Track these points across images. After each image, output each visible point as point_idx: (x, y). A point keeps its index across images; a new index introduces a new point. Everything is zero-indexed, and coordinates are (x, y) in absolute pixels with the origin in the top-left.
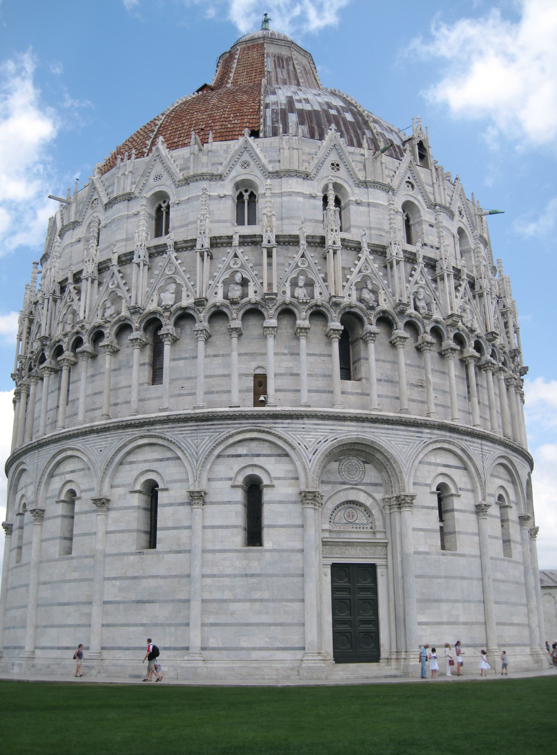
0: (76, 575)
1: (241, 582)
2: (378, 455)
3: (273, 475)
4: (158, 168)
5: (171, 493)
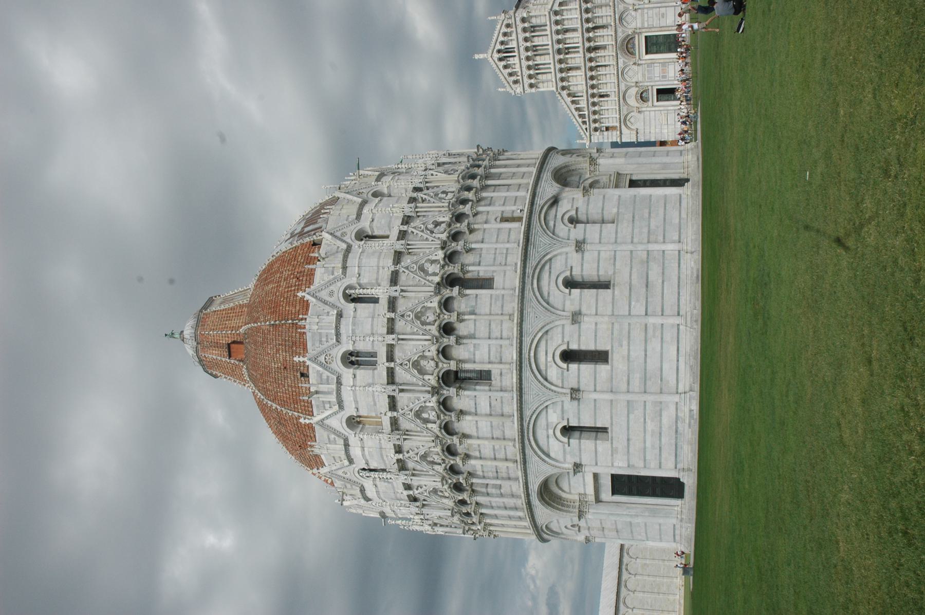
0: (625, 343)
1: (637, 223)
2: (563, 171)
3: (569, 208)
4: (324, 295)
5: (574, 265)
